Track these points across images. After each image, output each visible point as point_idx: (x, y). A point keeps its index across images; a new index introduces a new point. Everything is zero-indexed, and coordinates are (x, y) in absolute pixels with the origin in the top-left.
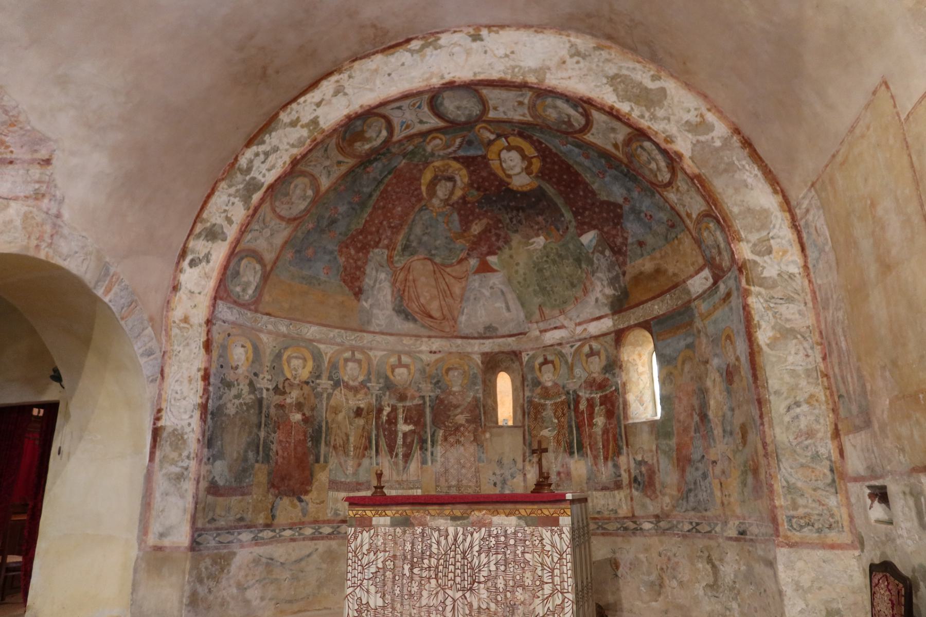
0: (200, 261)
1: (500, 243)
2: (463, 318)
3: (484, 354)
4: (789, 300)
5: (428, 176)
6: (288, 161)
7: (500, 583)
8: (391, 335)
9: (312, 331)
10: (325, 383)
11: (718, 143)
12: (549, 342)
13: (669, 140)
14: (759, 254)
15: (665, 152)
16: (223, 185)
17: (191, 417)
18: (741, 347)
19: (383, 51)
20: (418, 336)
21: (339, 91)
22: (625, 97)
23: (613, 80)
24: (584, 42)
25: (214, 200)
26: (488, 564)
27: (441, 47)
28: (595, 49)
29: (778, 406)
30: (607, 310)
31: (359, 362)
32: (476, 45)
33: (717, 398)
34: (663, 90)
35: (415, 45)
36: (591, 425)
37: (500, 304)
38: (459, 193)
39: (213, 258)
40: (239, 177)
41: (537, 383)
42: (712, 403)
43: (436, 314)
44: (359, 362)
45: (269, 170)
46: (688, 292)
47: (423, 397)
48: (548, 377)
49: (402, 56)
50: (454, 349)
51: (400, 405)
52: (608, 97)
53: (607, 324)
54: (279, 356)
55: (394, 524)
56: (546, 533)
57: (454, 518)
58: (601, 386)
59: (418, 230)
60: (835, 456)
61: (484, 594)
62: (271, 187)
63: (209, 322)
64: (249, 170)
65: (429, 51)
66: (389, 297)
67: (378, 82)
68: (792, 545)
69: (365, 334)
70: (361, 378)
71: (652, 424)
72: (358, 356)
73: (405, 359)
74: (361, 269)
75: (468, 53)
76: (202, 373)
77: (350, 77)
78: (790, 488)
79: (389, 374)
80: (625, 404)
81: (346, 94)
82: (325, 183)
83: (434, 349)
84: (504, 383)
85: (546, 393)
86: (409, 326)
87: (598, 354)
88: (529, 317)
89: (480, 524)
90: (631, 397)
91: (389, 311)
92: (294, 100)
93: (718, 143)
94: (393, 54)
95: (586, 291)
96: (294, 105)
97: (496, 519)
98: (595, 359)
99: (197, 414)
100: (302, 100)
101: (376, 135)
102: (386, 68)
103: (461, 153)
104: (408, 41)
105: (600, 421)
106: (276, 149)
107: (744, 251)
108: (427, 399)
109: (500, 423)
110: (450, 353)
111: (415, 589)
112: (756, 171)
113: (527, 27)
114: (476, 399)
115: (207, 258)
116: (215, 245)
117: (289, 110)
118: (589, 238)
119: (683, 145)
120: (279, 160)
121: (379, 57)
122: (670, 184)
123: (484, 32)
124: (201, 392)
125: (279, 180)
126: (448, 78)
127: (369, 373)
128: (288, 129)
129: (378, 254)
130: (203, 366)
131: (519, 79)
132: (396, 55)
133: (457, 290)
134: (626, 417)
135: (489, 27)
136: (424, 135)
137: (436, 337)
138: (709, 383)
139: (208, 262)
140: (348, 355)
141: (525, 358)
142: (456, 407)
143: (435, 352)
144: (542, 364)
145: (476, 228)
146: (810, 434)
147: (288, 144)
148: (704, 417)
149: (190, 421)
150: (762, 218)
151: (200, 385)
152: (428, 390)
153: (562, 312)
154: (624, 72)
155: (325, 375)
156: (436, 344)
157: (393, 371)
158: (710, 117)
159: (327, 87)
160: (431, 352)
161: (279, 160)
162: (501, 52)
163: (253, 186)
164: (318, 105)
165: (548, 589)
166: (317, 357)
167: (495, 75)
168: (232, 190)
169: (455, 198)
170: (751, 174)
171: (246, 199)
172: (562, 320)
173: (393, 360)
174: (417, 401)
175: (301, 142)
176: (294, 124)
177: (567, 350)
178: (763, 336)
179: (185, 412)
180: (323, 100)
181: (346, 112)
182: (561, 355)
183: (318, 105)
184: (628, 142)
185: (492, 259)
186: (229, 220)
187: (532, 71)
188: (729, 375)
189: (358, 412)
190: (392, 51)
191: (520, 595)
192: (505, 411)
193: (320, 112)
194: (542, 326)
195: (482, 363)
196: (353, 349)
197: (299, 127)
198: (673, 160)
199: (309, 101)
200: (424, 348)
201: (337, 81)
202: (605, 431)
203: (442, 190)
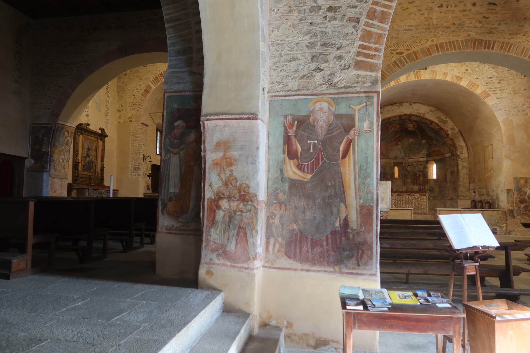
2: (390, 155)
4: (465, 162)
5: (391, 127)
7: (416, 204)
11: (456, 133)
12: (411, 161)
13: (447, 131)
14: (461, 154)
15: (446, 133)
18: (456, 169)
22: (440, 122)
23: (438, 118)
24: (433, 109)
26: (414, 201)
27: (403, 106)
28: (435, 110)
29: (461, 179)
30: (425, 156)
32: (411, 106)
33: (449, 176)
34: (447, 121)
35: (398, 104)
36: (419, 179)
38: (396, 129)
41: (406, 170)
42: (448, 177)
43: (384, 154)
46: (445, 156)
48: (409, 169)
49: (395, 107)
52: (437, 121)
53: (425, 159)
55: (397, 195)
56: (424, 197)
57: (408, 195)
58: (422, 172)
60: (469, 187)
61: (414, 205)
65: (401, 106)
67: (390, 112)
68: (460, 199)
71: (434, 180)
75: (409, 108)
77: (384, 110)
78: (461, 191)
80: (428, 176)
84: (396, 169)
85: (409, 172)
87: (422, 165)
88: (405, 156)
89: (413, 195)
90: (429, 174)
93: (456, 133)
95: (421, 152)
97: (416, 195)
98: (421, 166)
104: (396, 103)
105: (421, 178)
107: (458, 153)
111: (401, 205)
112: (462, 138)
113: (421, 103)
114: (392, 173)
118: (423, 141)
119: (450, 132)
121: (390, 106)
122: (446, 137)
123: (412, 104)
126: (405, 113)
131: (420, 115)
134: (428, 178)
135: (413, 102)
136: (395, 121)
138: (447, 173)
141: (404, 164)
144: (408, 166)
145: (397, 136)
146: (465, 183)
148: (446, 179)
150: (462, 147)
153: (414, 155)
154: (440, 116)
158: (455, 127)
162: (416, 109)
165: (424, 205)
167: (415, 114)
170: (461, 139)
172: (414, 157)
177: (414, 163)
178: (460, 167)
182: (413, 164)
184: (439, 129)
185: (399, 142)
187: (423, 114)
188: (452, 173)
191: (419, 205)
192: (396, 175)
194: (409, 157)
198: (447, 135)
202: (423, 180)
203: (392, 129)
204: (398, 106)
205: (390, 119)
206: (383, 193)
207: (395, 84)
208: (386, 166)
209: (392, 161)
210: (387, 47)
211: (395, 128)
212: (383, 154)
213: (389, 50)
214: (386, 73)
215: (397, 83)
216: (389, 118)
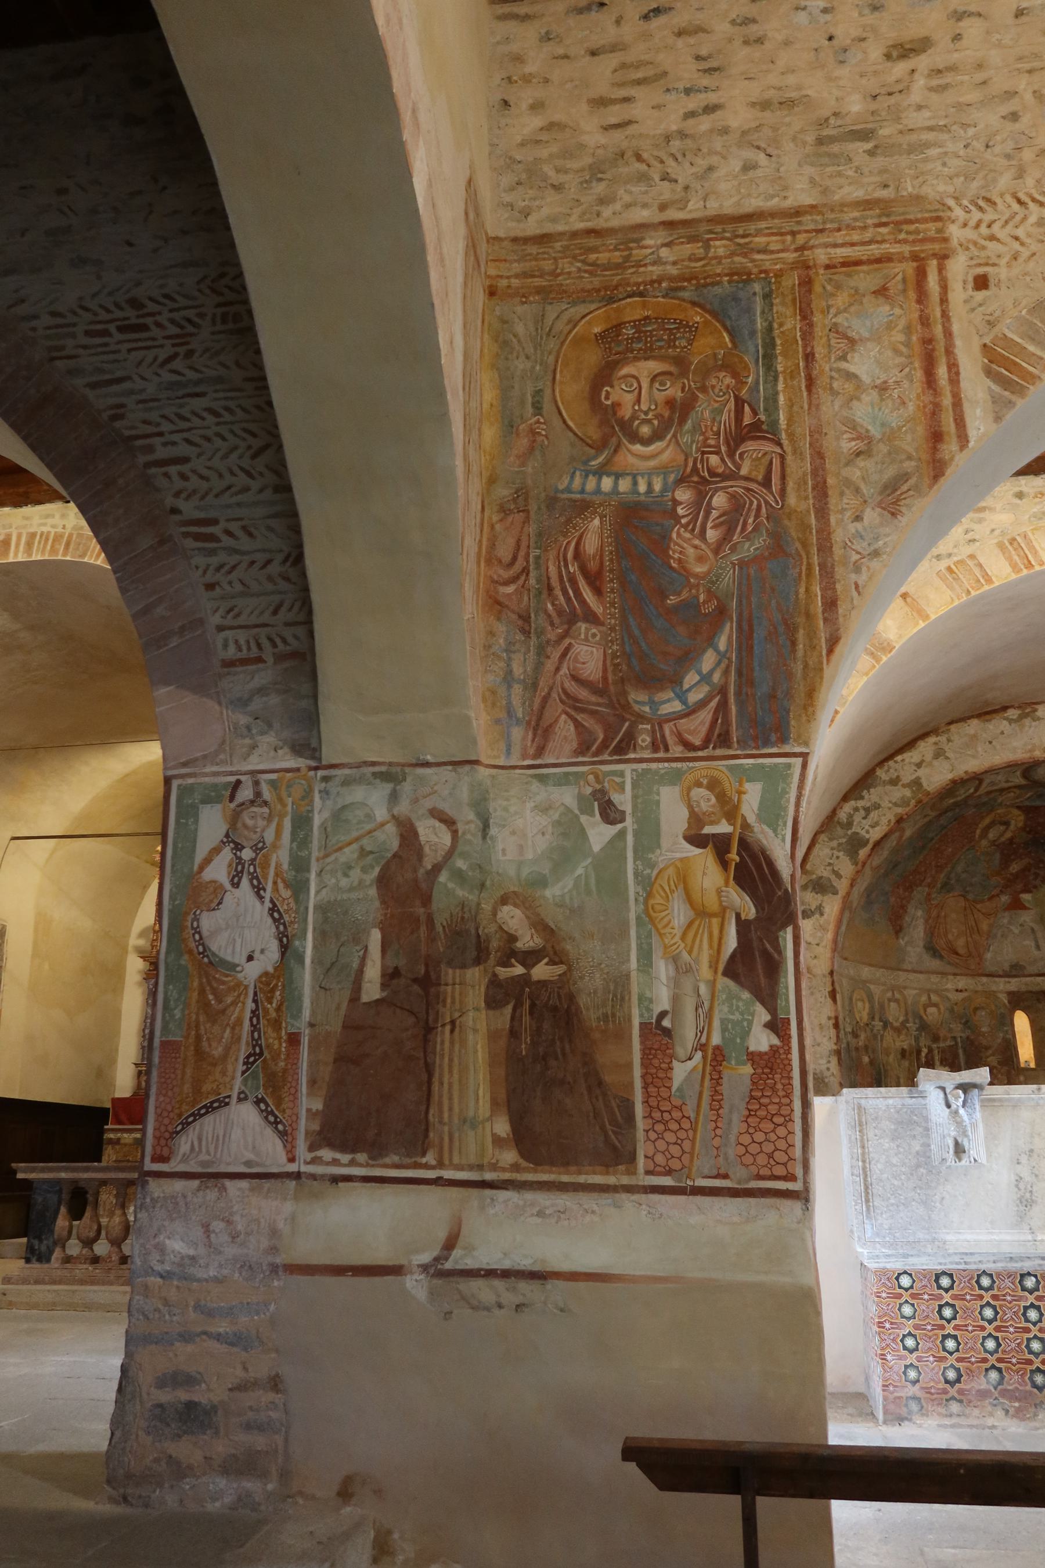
0: (813, 913)
1: (1038, 882)
2: (988, 956)
3: (1010, 994)
5: (987, 821)
6: (893, 821)
8: (921, 972)
9: (866, 972)
10: (878, 1024)
16: (823, 837)
17: (829, 1062)
19: (979, 716)
20: (943, 974)
21: (939, 754)
25: (816, 851)
27: (1039, 719)
31: (897, 1001)
35: (1012, 713)
37: (1029, 943)
38: (1008, 835)
39: (827, 910)
40: (839, 831)
43: (961, 951)
44: (897, 1001)
45: (872, 827)
47: (954, 1038)
49: (999, 725)
50: (980, 988)
51: (935, 1046)
54: (851, 999)
59: (959, 869)
62: (878, 844)
63: (831, 973)
64: (849, 824)
65: (1027, 721)
66: (922, 934)
67: (980, 749)
69: (901, 973)
70: (901, 1019)
72: (897, 996)
73: (934, 998)
74: (903, 907)
76: (833, 1021)
77: (949, 740)
79: (922, 1012)
81: (947, 758)
82: (908, 833)
83: (960, 987)
84: (1022, 1022)
86: (935, 964)
91: (920, 949)
92: (891, 757)
94: (990, 720)
96: (891, 763)
99: (834, 1060)
100: (899, 758)
101: (962, 794)
102: (984, 735)
103: (1028, 803)
104: (1005, 708)
106: (877, 806)
108: (959, 1040)
109: (1022, 1065)
110: (976, 992)
115: (820, 910)
116: (826, 898)
117: (886, 768)
120: (883, 818)
121: (975, 722)
124: (834, 1039)
125: (885, 837)
127: (907, 1014)
128: (889, 788)
129: (920, 892)
130: (833, 1015)
132: (993, 722)
133: (984, 926)
137: (961, 975)
139: (822, 914)
140: (889, 994)
142: (987, 1048)
143: (961, 991)
145: (1015, 867)
147: (890, 802)
149: (829, 1065)
151: (833, 1032)
152: (958, 1030)
155: (877, 1018)
156: (962, 982)
157: (925, 1011)
159: (925, 748)
160: (957, 990)
161: (883, 818)
163: (855, 844)
164: (919, 765)
166: (870, 997)
168: (834, 843)
169: (1003, 839)
171: (852, 853)
173: (924, 999)
174: (949, 1043)
175: (904, 802)
176: (894, 782)
179: (822, 1058)
180: (923, 761)
181: (950, 776)
183: (919, 765)
185: (1026, 897)
186: (839, 876)
189: (903, 1053)
190: (988, 717)
193: (921, 773)
195: (1009, 1002)
196: (893, 989)
197: (899, 786)
199: (907, 761)
200: (949, 986)
201: (936, 743)
203: (992, 835)
204: (1016, 721)
205: (981, 781)
206: (1024, 1159)
207: (1014, 576)
208: (976, 1009)
209: (1003, 986)
210: (1020, 202)
211: (1002, 828)
212: (957, 954)
213: (1033, 219)
214: (1031, 348)
215: (1025, 572)
216: (977, 778)
